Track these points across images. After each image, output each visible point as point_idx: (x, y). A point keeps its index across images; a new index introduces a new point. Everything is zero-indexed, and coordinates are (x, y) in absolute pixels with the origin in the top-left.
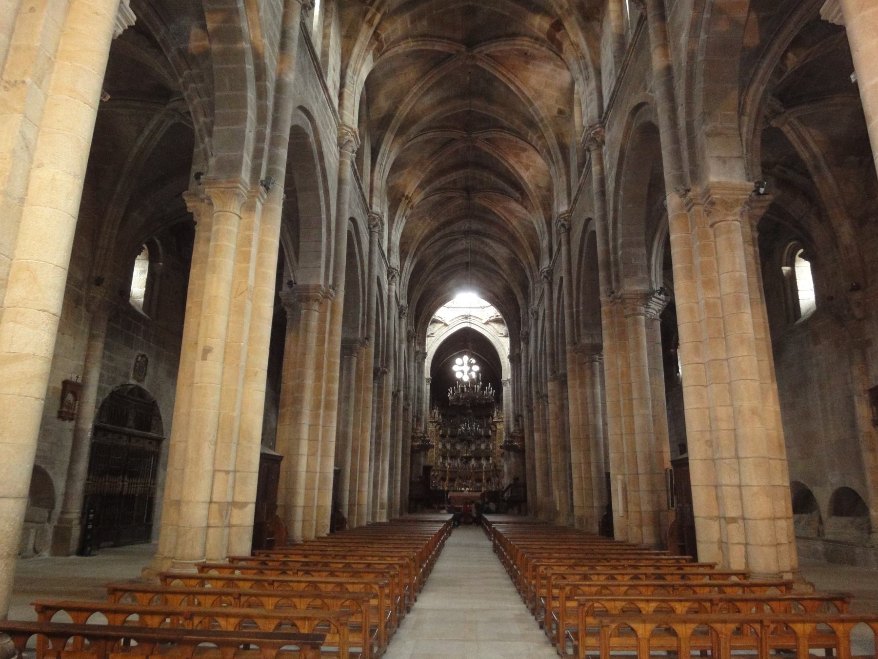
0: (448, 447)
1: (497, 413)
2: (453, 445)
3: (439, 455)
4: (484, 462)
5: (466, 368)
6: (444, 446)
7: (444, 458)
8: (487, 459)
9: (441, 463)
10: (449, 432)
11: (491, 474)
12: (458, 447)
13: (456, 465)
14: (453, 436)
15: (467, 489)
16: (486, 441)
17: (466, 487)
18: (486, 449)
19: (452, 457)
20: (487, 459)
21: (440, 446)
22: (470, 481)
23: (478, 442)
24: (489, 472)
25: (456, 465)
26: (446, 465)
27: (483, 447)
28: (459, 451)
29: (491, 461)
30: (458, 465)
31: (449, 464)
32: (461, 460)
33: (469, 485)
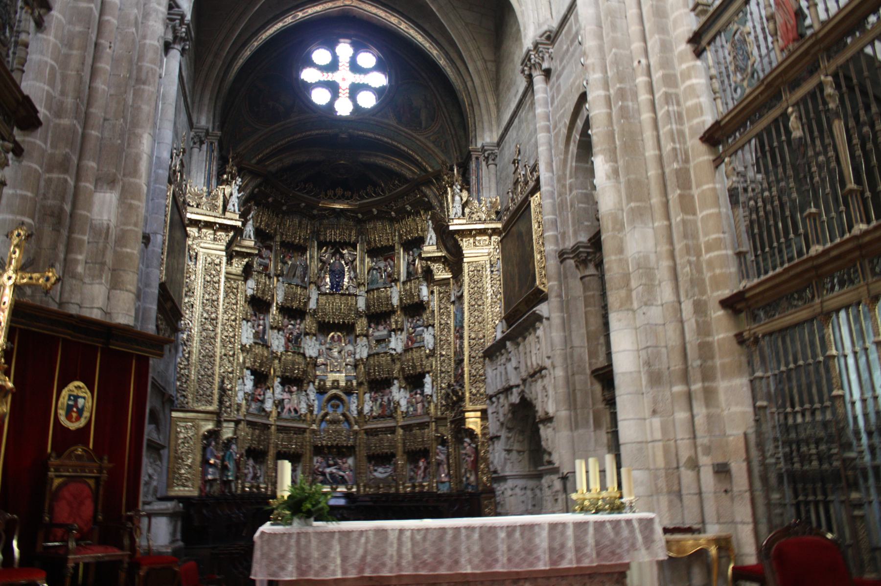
0: (277, 342)
1: (464, 206)
2: (294, 342)
3: (243, 366)
4: (399, 395)
5: (344, 77)
6: (260, 339)
7: (261, 379)
8: (414, 382)
9: (251, 398)
10: (279, 298)
11: (431, 432)
12: (311, 347)
13: (303, 409)
14: (292, 312)
15: (342, 489)
16: (407, 325)
17: (336, 481)
18: (407, 350)
19: (286, 382)
20: (414, 382)
21: (247, 335)
22: (350, 461)
23: (382, 332)
24: (423, 426)
25: (303, 409)
26: (269, 406)
27: (397, 344)
28: (314, 363)
29: (428, 389)
30: (310, 407)
31: (279, 404)
32: (321, 391)
33: (347, 474)
